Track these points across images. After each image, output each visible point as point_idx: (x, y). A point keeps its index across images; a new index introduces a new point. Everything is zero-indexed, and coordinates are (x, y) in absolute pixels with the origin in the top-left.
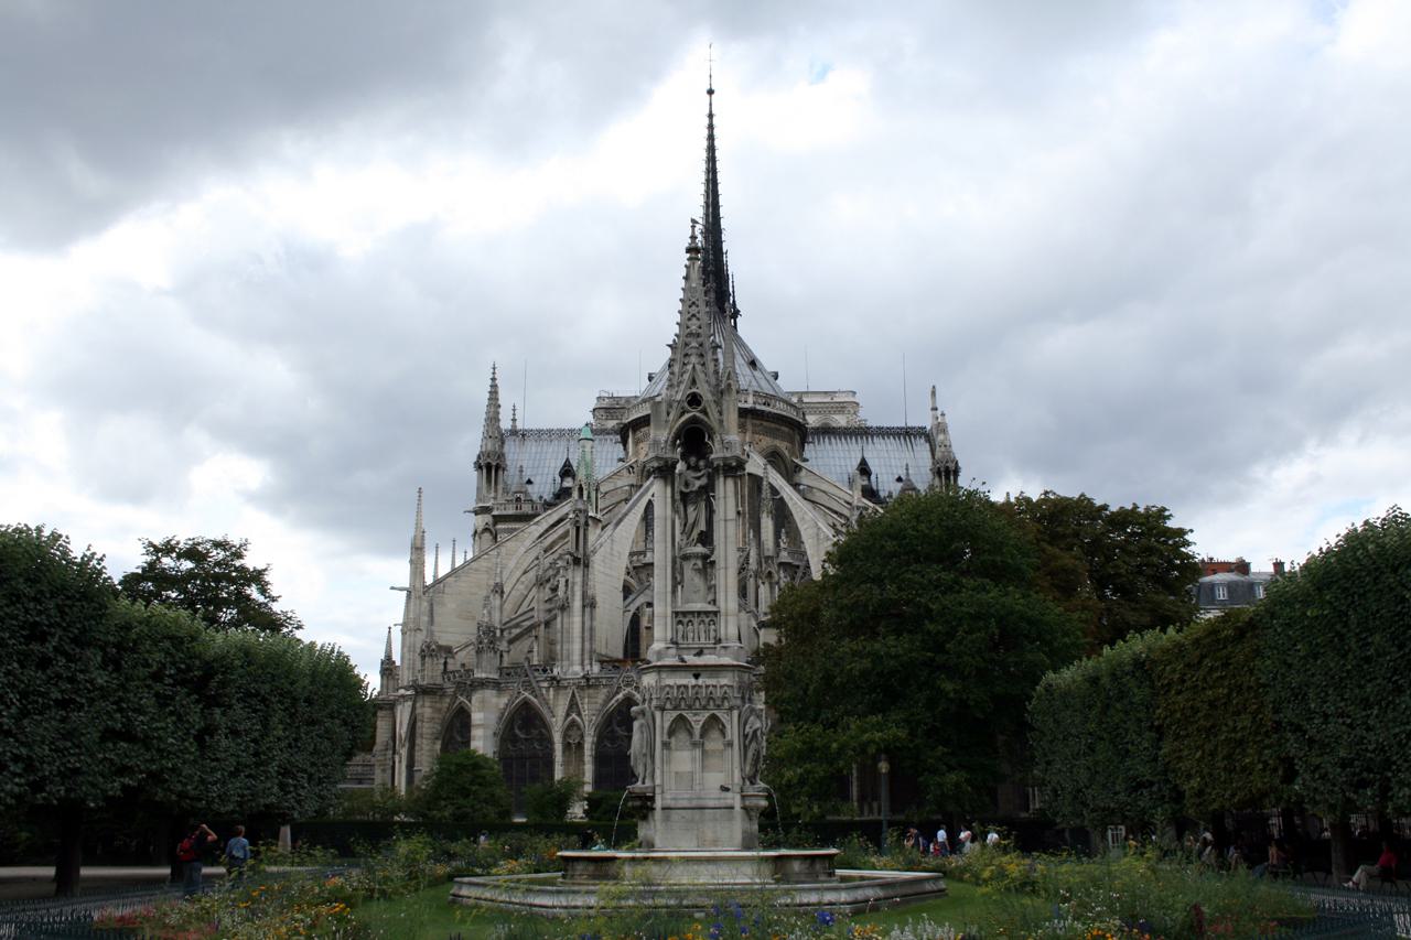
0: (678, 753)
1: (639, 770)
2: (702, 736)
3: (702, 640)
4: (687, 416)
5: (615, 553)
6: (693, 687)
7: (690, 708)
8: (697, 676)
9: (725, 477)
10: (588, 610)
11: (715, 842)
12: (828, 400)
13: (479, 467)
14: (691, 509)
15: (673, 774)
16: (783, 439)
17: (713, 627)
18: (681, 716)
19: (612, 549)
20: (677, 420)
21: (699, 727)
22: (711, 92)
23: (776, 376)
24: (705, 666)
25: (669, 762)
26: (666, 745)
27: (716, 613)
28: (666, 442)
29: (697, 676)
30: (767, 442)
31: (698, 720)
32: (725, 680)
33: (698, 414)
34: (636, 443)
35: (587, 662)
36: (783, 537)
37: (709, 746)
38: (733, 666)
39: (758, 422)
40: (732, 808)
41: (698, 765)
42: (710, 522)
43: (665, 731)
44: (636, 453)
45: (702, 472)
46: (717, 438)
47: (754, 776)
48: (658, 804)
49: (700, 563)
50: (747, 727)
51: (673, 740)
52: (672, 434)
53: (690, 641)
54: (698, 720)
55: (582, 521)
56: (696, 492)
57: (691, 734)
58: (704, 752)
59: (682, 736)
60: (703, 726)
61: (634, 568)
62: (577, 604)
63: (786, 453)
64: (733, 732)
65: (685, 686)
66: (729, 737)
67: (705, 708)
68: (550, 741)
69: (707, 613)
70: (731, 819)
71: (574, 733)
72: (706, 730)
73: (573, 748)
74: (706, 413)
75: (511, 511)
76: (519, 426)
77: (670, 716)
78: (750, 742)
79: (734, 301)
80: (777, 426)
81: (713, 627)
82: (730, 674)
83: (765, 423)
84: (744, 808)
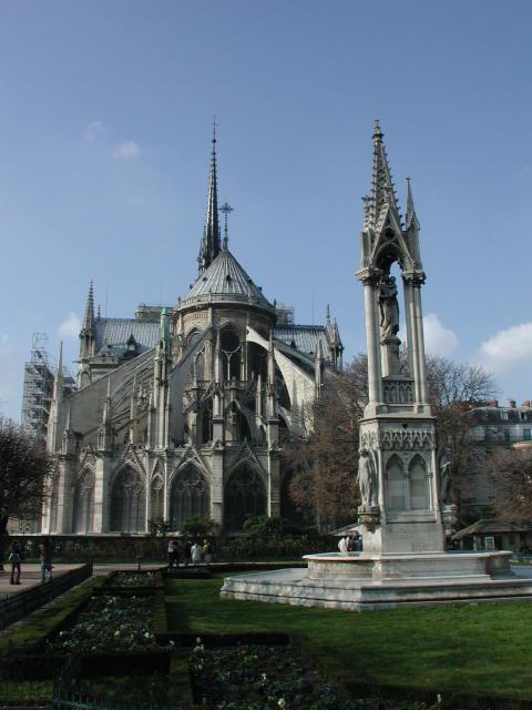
2: (410, 470)
3: (403, 398)
4: (385, 244)
6: (404, 434)
7: (402, 449)
8: (405, 426)
10: (167, 412)
11: (425, 547)
13: (81, 337)
18: (395, 456)
22: (214, 141)
26: (385, 476)
30: (257, 324)
31: (406, 458)
32: (423, 430)
34: (183, 323)
35: (166, 442)
37: (415, 477)
40: (435, 522)
41: (407, 493)
54: (406, 458)
55: (164, 362)
57: (401, 468)
58: (411, 482)
59: (395, 470)
62: (162, 408)
64: (432, 468)
67: (412, 450)
68: (143, 487)
69: (405, 382)
71: (159, 484)
73: (156, 494)
74: (397, 243)
75: (100, 362)
76: (103, 316)
77: (389, 454)
82: (428, 425)
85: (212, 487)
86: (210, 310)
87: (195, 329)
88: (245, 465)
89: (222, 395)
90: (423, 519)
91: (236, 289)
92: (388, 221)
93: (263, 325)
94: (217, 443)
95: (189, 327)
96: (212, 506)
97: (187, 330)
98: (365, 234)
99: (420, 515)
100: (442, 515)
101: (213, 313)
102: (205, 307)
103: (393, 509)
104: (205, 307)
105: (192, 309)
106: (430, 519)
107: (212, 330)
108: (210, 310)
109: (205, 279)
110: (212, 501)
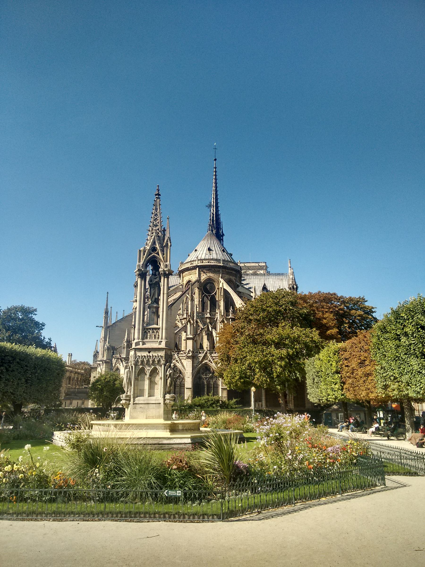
0: (141, 382)
1: (126, 390)
5: (172, 314)
8: (149, 352)
9: (164, 278)
12: (257, 265)
14: (152, 289)
15: (139, 391)
16: (233, 276)
17: (157, 334)
19: (171, 313)
20: (148, 257)
21: (149, 372)
23: (231, 255)
24: (153, 348)
25: (137, 385)
27: (159, 329)
28: (143, 265)
29: (149, 352)
30: (227, 277)
31: (148, 370)
33: (155, 255)
36: (231, 309)
38: (163, 348)
39: (224, 270)
40: (160, 404)
42: (159, 295)
43: (137, 373)
44: (183, 281)
45: (157, 277)
46: (162, 264)
47: (170, 391)
48: (132, 402)
49: (154, 310)
50: (168, 371)
51: (140, 377)
52: (145, 262)
53: (149, 339)
56: (154, 283)
60: (151, 372)
61: (180, 319)
63: (234, 281)
65: (145, 356)
66: (160, 376)
69: (156, 329)
70: (159, 408)
72: (153, 373)
74: (159, 255)
78: (168, 378)
79: (222, 231)
80: (231, 271)
81: (157, 334)
83: (227, 270)
84: (165, 404)
85: (186, 379)
86: (197, 269)
87: (189, 281)
88: (206, 364)
89: (192, 322)
90: (154, 402)
91: (215, 256)
92: (154, 243)
93: (231, 277)
94: (189, 351)
95: (186, 279)
96: (186, 389)
97: (185, 282)
98: (140, 251)
99: (152, 400)
100: (165, 400)
101: (199, 270)
102: (194, 268)
103: (137, 397)
104: (194, 268)
105: (187, 269)
106: (157, 402)
107: (198, 281)
108: (197, 269)
109: (196, 250)
110: (186, 387)
